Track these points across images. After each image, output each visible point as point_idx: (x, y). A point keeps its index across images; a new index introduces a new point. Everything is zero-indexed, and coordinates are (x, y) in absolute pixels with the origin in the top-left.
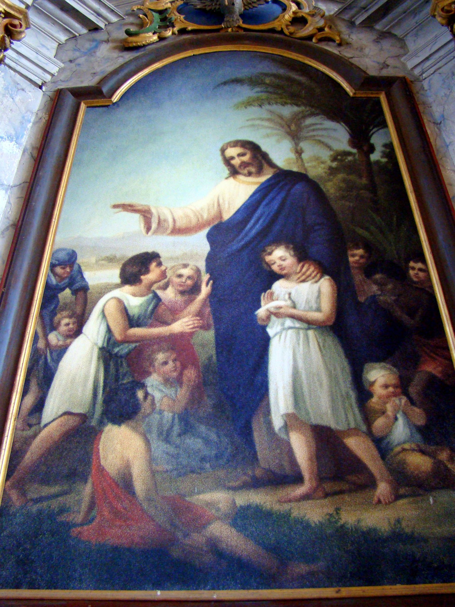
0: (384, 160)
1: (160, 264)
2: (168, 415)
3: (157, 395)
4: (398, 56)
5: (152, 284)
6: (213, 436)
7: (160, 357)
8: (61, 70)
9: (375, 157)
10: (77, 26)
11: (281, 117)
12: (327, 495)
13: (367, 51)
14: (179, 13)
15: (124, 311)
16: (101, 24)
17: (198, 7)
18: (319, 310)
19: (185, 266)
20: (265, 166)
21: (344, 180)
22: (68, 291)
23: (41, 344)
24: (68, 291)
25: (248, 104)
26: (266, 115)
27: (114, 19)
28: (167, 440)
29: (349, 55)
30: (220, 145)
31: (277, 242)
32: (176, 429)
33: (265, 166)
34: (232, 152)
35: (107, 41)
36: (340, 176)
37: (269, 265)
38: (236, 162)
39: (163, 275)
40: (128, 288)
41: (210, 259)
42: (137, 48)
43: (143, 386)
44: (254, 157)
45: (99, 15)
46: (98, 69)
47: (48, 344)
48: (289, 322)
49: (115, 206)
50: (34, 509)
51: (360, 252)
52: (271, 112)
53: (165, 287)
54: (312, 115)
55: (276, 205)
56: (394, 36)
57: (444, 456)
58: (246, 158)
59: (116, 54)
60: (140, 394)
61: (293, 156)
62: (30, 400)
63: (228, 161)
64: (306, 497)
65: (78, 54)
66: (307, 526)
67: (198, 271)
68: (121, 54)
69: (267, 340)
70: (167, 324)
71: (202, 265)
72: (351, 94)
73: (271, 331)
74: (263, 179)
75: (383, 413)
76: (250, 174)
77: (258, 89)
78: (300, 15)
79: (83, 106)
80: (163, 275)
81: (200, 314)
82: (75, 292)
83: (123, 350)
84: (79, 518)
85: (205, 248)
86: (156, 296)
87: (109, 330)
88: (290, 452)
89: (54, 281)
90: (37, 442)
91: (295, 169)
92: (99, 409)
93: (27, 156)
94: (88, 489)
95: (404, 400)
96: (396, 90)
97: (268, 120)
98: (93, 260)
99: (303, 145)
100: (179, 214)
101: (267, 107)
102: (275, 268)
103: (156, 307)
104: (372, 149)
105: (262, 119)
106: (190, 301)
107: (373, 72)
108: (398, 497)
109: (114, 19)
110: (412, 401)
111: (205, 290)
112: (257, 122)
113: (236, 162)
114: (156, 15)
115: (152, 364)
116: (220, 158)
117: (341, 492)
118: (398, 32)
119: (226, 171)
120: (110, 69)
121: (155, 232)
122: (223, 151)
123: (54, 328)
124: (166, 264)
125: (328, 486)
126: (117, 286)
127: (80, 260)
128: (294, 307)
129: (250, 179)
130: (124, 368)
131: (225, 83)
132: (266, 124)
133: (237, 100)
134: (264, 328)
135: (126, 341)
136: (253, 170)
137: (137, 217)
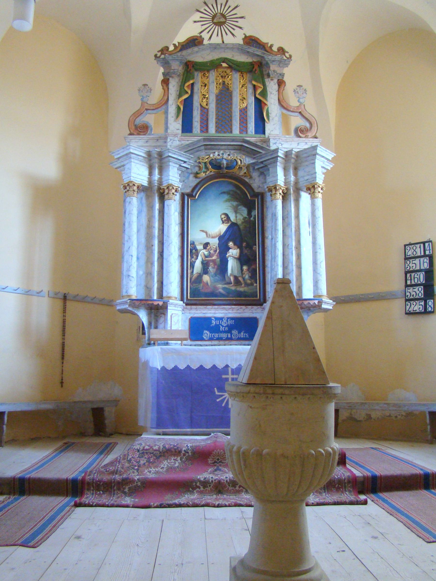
0: (253, 220)
1: (210, 245)
2: (213, 273)
3: (211, 270)
4: (263, 183)
5: (209, 249)
6: (219, 277)
7: (211, 263)
8: (182, 185)
9: (252, 219)
10: (184, 168)
11: (233, 205)
12: (235, 286)
13: (256, 181)
14: (209, 164)
15: (204, 255)
16: (189, 167)
17: (215, 164)
18: (237, 255)
19: (214, 246)
20: (229, 221)
21: (245, 225)
22: (194, 250)
23: (191, 261)
24: (194, 250)
25: (226, 201)
26: (230, 205)
27: (192, 164)
28: (213, 277)
29: (251, 183)
30: (220, 214)
31: (231, 241)
32: (214, 276)
33: (229, 221)
34: (223, 216)
35: (192, 173)
36: (244, 224)
37: (229, 246)
38: (223, 219)
39: (211, 247)
40: (204, 250)
41: (218, 244)
42: (199, 178)
43: (209, 268)
44: (227, 218)
45: (189, 164)
46: (191, 185)
47: (192, 261)
48: (232, 258)
49: (200, 231)
50: (195, 287)
51: (245, 243)
52: (231, 204)
53: (211, 250)
54: (240, 205)
55: (231, 231)
56: (264, 174)
57: (253, 281)
58: (225, 218)
59: (194, 179)
60: (208, 270)
61: (235, 218)
62: (191, 271)
63: (222, 219)
64: (232, 286)
65: (185, 178)
66: (232, 290)
67: (217, 247)
68: (196, 179)
69: (227, 261)
70: (212, 257)
71: (217, 245)
72: (249, 198)
73: (229, 259)
74: (229, 224)
75: (245, 274)
76: (226, 223)
77: (228, 196)
78: (241, 166)
79: (189, 200)
80: (211, 247)
81: (217, 256)
82: (195, 251)
83: (205, 262)
84: (201, 288)
85: (218, 242)
86: (210, 252)
87: (202, 258)
88: (231, 279)
89: (191, 248)
90: (193, 278)
91: (235, 222)
92: (202, 273)
93: (180, 215)
94: (202, 285)
95: (248, 272)
96: (260, 197)
97: (231, 206)
98: (198, 243)
99: (238, 215)
100: (213, 233)
101: (231, 202)
102: (230, 247)
103: (210, 255)
104: (251, 217)
105: (229, 206)
106: (215, 253)
107: (256, 190)
108: (245, 286)
109: (192, 164)
110: (249, 272)
111: (218, 251)
112: (228, 207)
113: (223, 219)
114: (203, 164)
115: (210, 264)
116: (220, 219)
117: (237, 285)
118: (265, 173)
119: (222, 222)
120: (194, 184)
121: (209, 237)
122: (221, 216)
123: (193, 257)
124: (211, 245)
125: (236, 285)
126: (203, 250)
127: (195, 243)
128: (233, 255)
129: (226, 225)
130: (205, 265)
131: (222, 193)
132: (230, 208)
133: (225, 199)
134: (227, 259)
135: (205, 260)
136: (227, 222)
137: (205, 234)
